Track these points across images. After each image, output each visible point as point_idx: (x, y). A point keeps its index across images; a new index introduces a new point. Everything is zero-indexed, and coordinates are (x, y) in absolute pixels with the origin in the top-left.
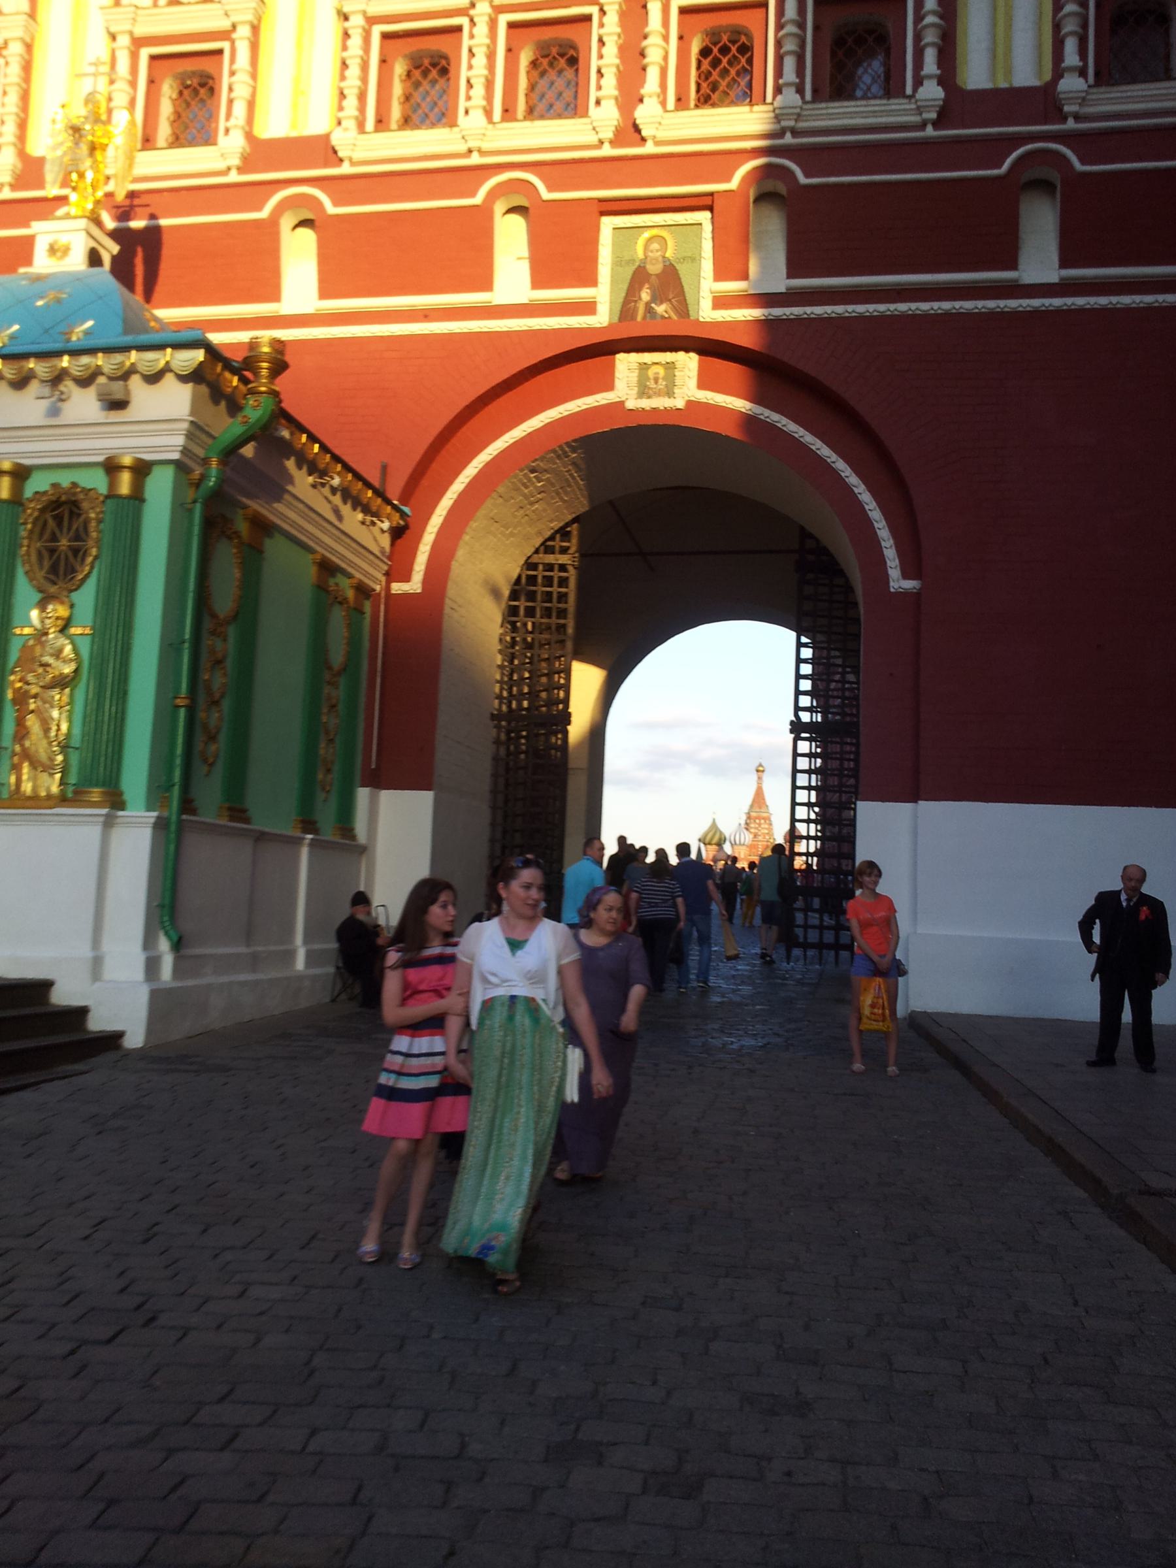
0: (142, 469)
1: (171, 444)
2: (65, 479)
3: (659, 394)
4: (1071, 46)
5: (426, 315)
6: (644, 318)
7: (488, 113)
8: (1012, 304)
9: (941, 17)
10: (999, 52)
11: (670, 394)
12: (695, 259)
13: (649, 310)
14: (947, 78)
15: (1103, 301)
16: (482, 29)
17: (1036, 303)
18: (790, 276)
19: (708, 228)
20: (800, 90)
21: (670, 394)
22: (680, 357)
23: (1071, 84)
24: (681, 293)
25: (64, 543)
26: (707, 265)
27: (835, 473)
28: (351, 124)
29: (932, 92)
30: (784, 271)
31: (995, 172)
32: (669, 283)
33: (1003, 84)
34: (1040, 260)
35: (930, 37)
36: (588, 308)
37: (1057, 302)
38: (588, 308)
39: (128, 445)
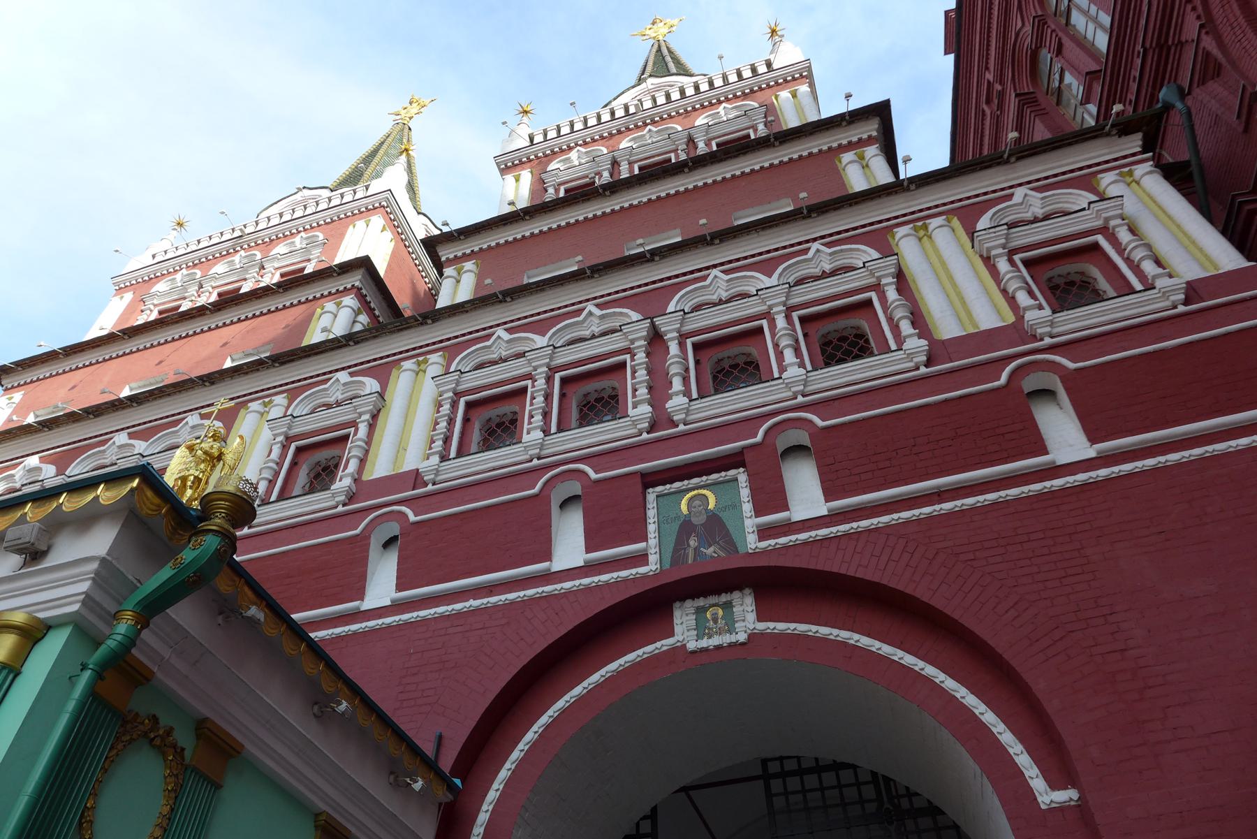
5: (491, 589)
6: (695, 560)
8: (1058, 483)
11: (731, 630)
12: (737, 506)
15: (1150, 462)
17: (1081, 477)
18: (827, 501)
19: (742, 476)
20: (802, 365)
21: (731, 630)
22: (736, 594)
26: (747, 508)
27: (928, 680)
30: (822, 498)
31: (996, 384)
32: (715, 528)
37: (1103, 473)
38: (642, 558)
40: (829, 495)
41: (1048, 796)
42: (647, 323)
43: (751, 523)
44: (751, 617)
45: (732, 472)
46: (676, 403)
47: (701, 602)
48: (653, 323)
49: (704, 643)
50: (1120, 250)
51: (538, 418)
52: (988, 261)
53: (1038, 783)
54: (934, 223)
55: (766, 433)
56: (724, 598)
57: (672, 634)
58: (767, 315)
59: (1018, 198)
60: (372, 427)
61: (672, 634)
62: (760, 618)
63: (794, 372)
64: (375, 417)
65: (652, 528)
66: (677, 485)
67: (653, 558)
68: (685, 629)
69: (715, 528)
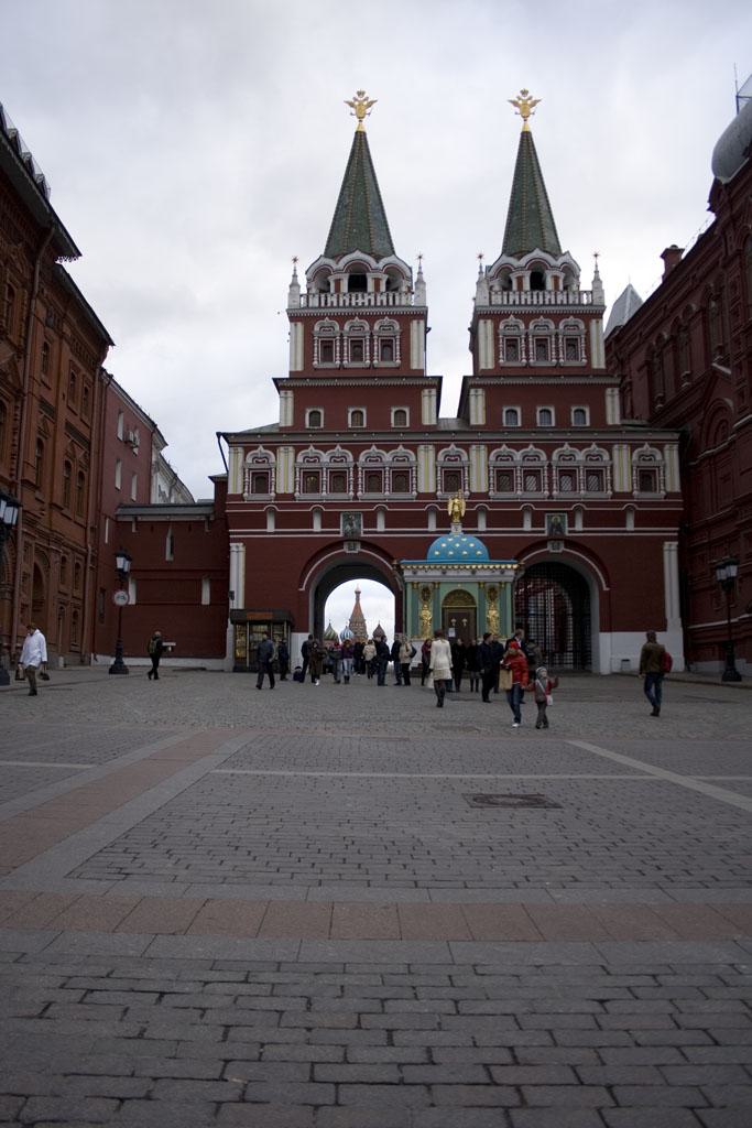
0: (506, 583)
1: (511, 579)
10: (621, 485)
14: (612, 490)
23: (635, 493)
29: (610, 492)
32: (559, 527)
34: (630, 526)
36: (543, 532)
38: (543, 532)
39: (503, 579)
40: (584, 526)
41: (605, 589)
43: (567, 529)
53: (604, 585)
54: (625, 446)
59: (645, 448)
63: (582, 492)
68: (549, 548)
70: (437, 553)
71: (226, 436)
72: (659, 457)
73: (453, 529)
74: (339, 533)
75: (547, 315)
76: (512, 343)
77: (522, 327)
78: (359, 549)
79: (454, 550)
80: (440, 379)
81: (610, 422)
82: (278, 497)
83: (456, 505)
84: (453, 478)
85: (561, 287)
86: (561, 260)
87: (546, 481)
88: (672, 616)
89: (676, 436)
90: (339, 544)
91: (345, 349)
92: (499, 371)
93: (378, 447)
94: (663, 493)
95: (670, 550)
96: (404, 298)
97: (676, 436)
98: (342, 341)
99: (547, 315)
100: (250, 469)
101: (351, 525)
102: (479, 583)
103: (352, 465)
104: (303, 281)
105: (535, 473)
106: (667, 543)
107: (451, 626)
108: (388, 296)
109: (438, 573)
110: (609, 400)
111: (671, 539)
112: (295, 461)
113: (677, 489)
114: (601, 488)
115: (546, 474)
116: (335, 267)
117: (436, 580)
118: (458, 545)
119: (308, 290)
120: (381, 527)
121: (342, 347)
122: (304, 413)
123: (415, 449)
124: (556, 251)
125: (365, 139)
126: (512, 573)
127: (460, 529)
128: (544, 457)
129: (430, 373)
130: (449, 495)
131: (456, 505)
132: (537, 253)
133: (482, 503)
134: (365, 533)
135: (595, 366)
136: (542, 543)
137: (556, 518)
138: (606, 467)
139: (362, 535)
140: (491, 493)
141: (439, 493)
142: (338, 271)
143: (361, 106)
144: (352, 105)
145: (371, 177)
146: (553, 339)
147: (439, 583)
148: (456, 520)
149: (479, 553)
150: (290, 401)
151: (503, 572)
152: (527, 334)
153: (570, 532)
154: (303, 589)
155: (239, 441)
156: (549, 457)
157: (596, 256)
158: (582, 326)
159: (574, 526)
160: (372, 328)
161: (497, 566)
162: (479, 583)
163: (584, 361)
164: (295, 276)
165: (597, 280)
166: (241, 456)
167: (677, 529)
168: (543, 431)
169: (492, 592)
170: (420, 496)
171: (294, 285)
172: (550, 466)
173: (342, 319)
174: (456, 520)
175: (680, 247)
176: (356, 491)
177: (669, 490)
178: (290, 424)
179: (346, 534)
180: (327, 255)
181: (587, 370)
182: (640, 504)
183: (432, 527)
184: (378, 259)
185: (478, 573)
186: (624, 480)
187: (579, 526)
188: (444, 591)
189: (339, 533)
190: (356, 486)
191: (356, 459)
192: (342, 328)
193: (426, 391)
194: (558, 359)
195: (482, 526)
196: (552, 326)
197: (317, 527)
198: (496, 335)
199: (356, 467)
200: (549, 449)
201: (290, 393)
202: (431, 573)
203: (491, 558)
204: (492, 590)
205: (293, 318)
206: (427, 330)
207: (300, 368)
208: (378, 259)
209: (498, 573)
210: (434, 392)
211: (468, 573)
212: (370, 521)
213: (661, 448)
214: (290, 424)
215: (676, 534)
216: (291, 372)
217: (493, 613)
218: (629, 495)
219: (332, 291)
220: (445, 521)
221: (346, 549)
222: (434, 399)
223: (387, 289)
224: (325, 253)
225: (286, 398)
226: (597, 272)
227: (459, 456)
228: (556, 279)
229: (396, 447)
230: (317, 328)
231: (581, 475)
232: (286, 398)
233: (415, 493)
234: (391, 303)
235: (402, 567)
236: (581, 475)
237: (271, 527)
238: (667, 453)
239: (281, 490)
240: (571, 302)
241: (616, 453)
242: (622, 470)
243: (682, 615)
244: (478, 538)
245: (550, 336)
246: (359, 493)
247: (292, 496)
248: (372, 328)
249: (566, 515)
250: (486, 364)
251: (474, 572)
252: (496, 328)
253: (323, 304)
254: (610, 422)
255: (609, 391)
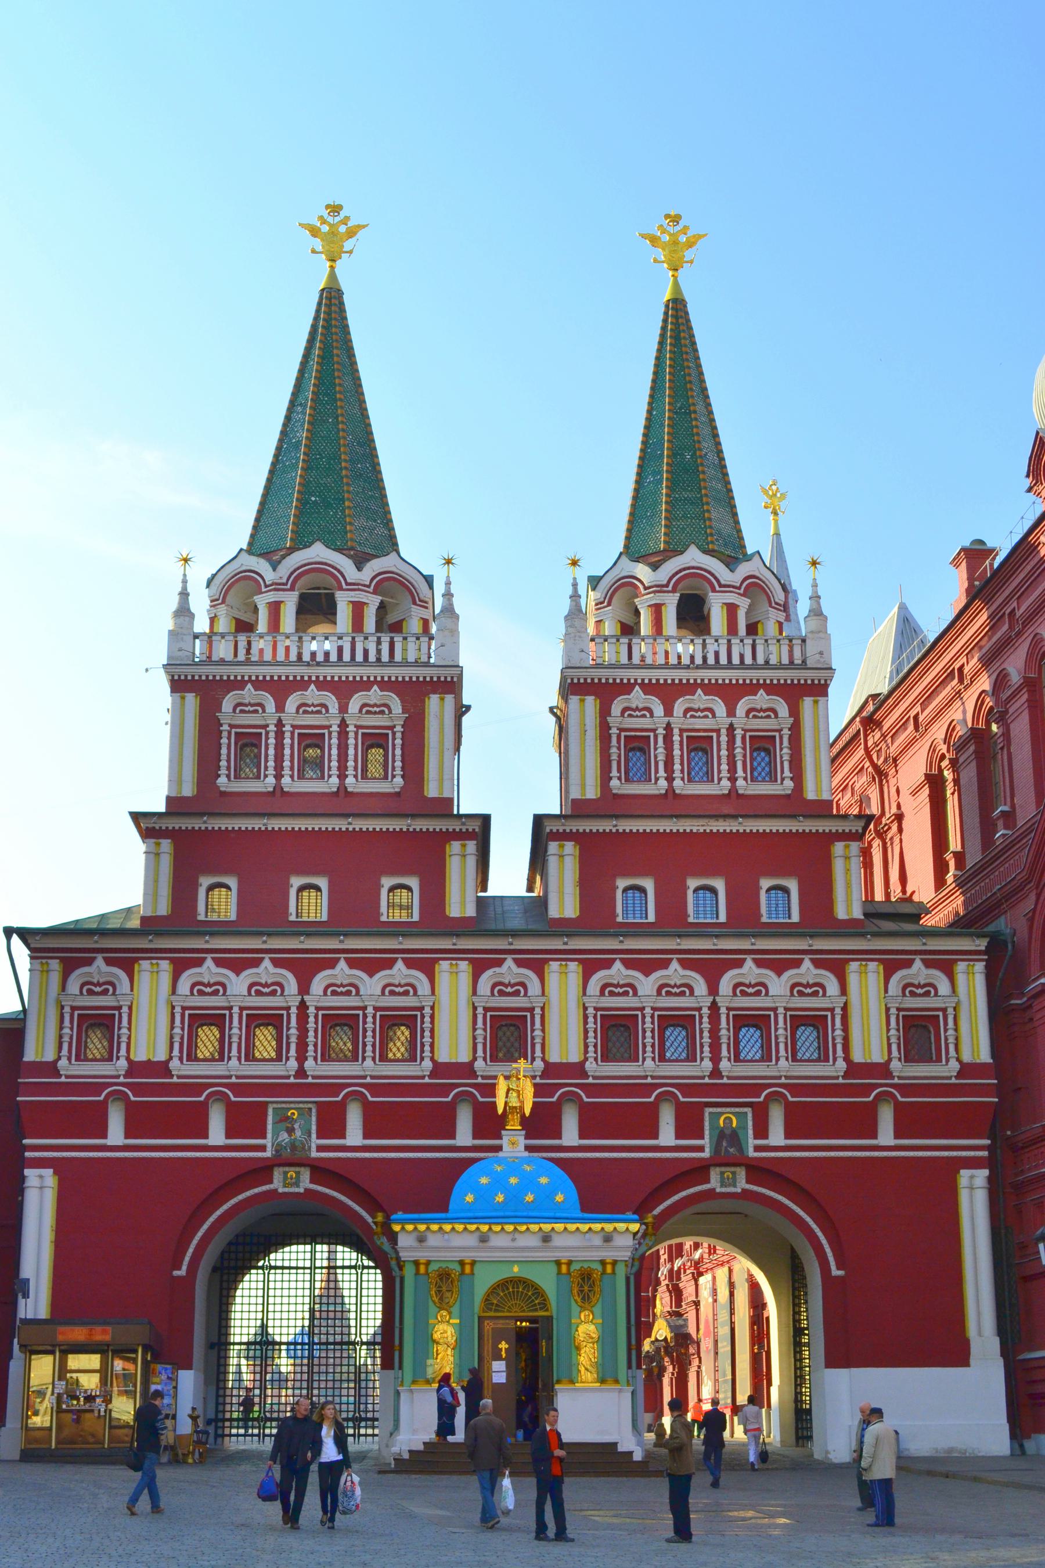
0: (614, 1263)
1: (626, 1255)
2: (586, 1265)
3: (730, 1185)
4: (894, 1047)
7: (653, 1059)
9: (843, 1030)
10: (866, 1046)
11: (735, 1186)
12: (746, 1128)
13: (726, 1150)
14: (847, 1059)
16: (648, 1019)
21: (735, 1186)
22: (738, 1169)
23: (895, 1065)
24: (738, 1140)
25: (586, 1288)
26: (750, 1132)
28: (591, 1060)
29: (841, 1065)
32: (733, 1137)
33: (869, 1061)
34: (886, 1135)
35: (839, 1040)
36: (701, 1149)
38: (701, 1149)
39: (609, 1255)
40: (787, 1137)
41: (836, 1272)
42: (711, 999)
43: (752, 1142)
44: (744, 1181)
45: (745, 1110)
46: (724, 1065)
47: (723, 1169)
48: (714, 1000)
49: (724, 1190)
50: (946, 1030)
51: (649, 1049)
52: (887, 1010)
54: (872, 965)
55: (766, 1096)
56: (733, 1169)
57: (708, 1181)
58: (775, 1009)
60: (543, 1017)
61: (708, 1181)
62: (748, 1182)
64: (543, 1009)
65: (707, 1133)
66: (719, 1110)
67: (707, 1150)
69: (733, 1137)
70: (470, 1198)
71: (25, 934)
72: (944, 988)
73: (505, 1142)
74: (263, 1148)
75: (710, 688)
76: (637, 744)
77: (659, 710)
78: (306, 1182)
79: (506, 1189)
80: (485, 820)
81: (841, 913)
82: (135, 1068)
83: (515, 1090)
84: (509, 1032)
85: (742, 629)
86: (744, 569)
87: (706, 1040)
88: (980, 1334)
89: (982, 944)
90: (262, 1171)
91: (287, 752)
92: (610, 804)
93: (352, 964)
94: (954, 1065)
95: (971, 1188)
96: (412, 646)
97: (982, 944)
98: (280, 735)
99: (710, 688)
100: (73, 1009)
101: (290, 1131)
102: (558, 1263)
103: (294, 1002)
104: (200, 604)
105: (685, 1021)
106: (964, 1176)
107: (498, 1358)
108: (379, 642)
109: (472, 1241)
110: (838, 867)
111: (973, 1164)
112: (174, 992)
113: (984, 1056)
114: (823, 1057)
115: (706, 1025)
116: (270, 576)
117: (467, 1256)
118: (513, 1181)
119: (212, 620)
120: (354, 1135)
121: (279, 747)
122: (196, 886)
123: (427, 967)
124: (733, 551)
125: (341, 304)
126: (629, 1241)
127: (522, 1141)
128: (701, 987)
129: (467, 805)
130: (498, 1069)
131: (515, 1090)
132: (694, 557)
133: (569, 1084)
134: (320, 1148)
135: (810, 794)
136: (699, 1171)
137: (729, 1118)
138: (832, 1010)
139: (314, 1154)
140: (590, 1066)
141: (479, 1064)
142: (277, 586)
143: (334, 235)
144: (314, 232)
145: (348, 383)
146: (724, 738)
147: (473, 1263)
148: (514, 1124)
149: (559, 1198)
150: (166, 862)
151: (608, 1238)
152: (668, 728)
153: (757, 1148)
154: (182, 1272)
155: (59, 949)
156: (713, 990)
157: (814, 563)
158: (783, 710)
159: (766, 1137)
160: (343, 709)
161: (597, 1227)
162: (558, 1263)
163: (789, 784)
164: (184, 594)
165: (816, 612)
166: (55, 978)
167: (988, 1142)
168: (701, 930)
169: (585, 1283)
170: (439, 1069)
171: (183, 612)
172: (714, 1007)
173: (281, 689)
174: (514, 1124)
175: (990, 544)
176: (301, 1058)
177: (966, 1058)
178: (163, 908)
179: (278, 1148)
180: (252, 549)
181: (795, 804)
182: (906, 1089)
183: (464, 1135)
184: (360, 563)
185: (557, 1241)
186: (871, 1039)
187: (777, 1136)
188: (483, 1282)
189: (263, 1148)
190: (302, 1047)
191: (304, 988)
192: (280, 707)
193: (455, 847)
194: (733, 779)
195: (570, 1134)
196: (721, 709)
197: (217, 1133)
198: (604, 728)
199: (303, 1007)
200: (712, 969)
201: (166, 845)
202: (457, 1241)
203: (584, 1209)
204: (586, 1276)
205: (179, 685)
206: (462, 710)
207: (188, 790)
208: (360, 563)
209: (597, 1241)
210: (471, 846)
211: (534, 1241)
212: (332, 1123)
213: (948, 969)
214: (163, 908)
215: (985, 1154)
216: (169, 799)
217: (586, 1329)
218: (882, 1070)
219: (262, 627)
220: (490, 1123)
221: (277, 1184)
222: (471, 862)
223: (379, 628)
224: (250, 544)
225: (158, 854)
226: (816, 598)
227: (523, 985)
228: (731, 610)
229: (389, 964)
230: (227, 705)
231: (781, 1031)
232: (158, 854)
233: (427, 1064)
234: (385, 657)
235: (397, 1228)
236: (781, 1031)
237: (116, 1133)
238: (961, 979)
239: (140, 1055)
240: (760, 660)
241: (852, 979)
242: (869, 1013)
243: (1001, 1331)
244: (557, 1162)
245: (718, 731)
246: (309, 1064)
247: (162, 1068)
248: (343, 709)
249: (749, 1111)
250: (583, 786)
251: (546, 1238)
252: (604, 712)
253: (241, 656)
254: (841, 913)
255: (838, 848)
